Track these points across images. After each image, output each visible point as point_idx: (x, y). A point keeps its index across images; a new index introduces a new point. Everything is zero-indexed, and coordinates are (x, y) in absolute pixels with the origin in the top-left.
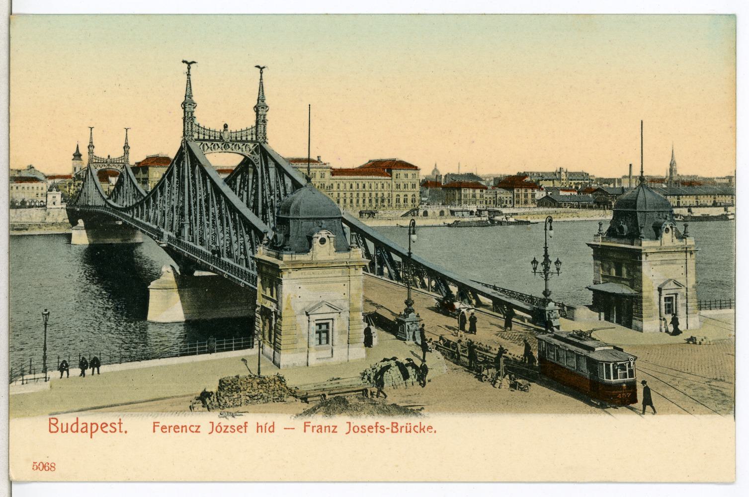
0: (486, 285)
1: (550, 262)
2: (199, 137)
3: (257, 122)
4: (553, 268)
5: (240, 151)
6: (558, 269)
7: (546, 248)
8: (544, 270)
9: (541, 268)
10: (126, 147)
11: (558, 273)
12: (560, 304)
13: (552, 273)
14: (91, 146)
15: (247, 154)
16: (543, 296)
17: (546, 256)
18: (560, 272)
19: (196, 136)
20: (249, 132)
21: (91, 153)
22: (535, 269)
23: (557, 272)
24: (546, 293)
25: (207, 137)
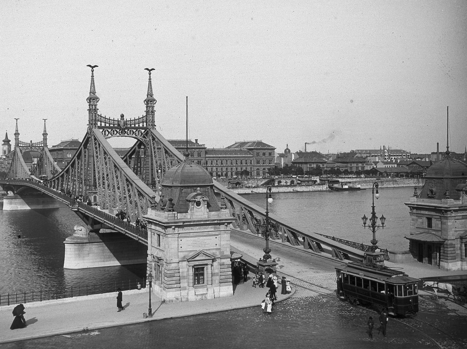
0: (327, 237)
1: (377, 218)
2: (101, 125)
3: (147, 112)
4: (379, 222)
5: (134, 135)
6: (383, 224)
7: (373, 207)
8: (371, 224)
9: (369, 223)
10: (45, 134)
11: (383, 227)
12: (384, 250)
13: (378, 226)
14: (17, 134)
15: (139, 137)
16: (371, 245)
17: (374, 213)
18: (384, 225)
19: (99, 124)
20: (141, 120)
21: (17, 139)
22: (365, 223)
23: (382, 225)
24: (374, 242)
25: (107, 125)
